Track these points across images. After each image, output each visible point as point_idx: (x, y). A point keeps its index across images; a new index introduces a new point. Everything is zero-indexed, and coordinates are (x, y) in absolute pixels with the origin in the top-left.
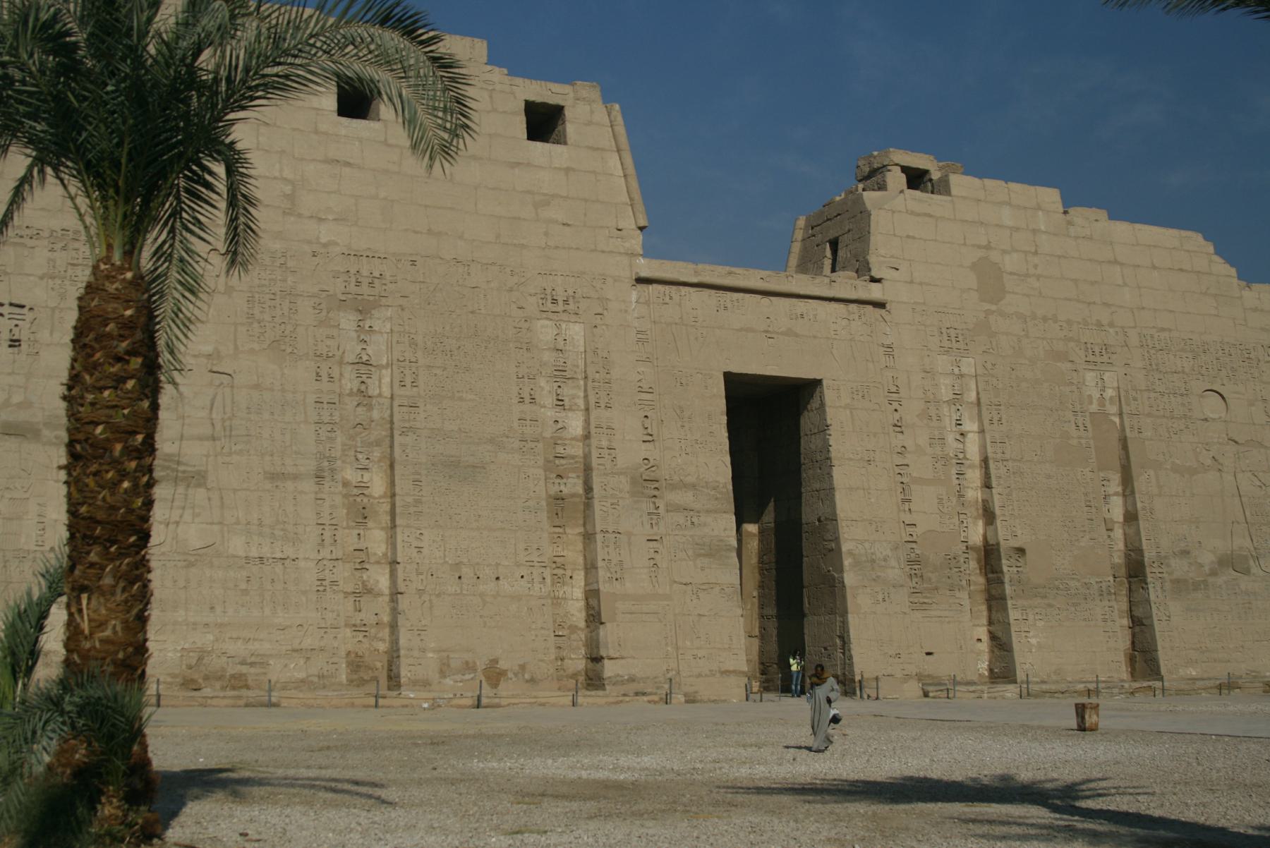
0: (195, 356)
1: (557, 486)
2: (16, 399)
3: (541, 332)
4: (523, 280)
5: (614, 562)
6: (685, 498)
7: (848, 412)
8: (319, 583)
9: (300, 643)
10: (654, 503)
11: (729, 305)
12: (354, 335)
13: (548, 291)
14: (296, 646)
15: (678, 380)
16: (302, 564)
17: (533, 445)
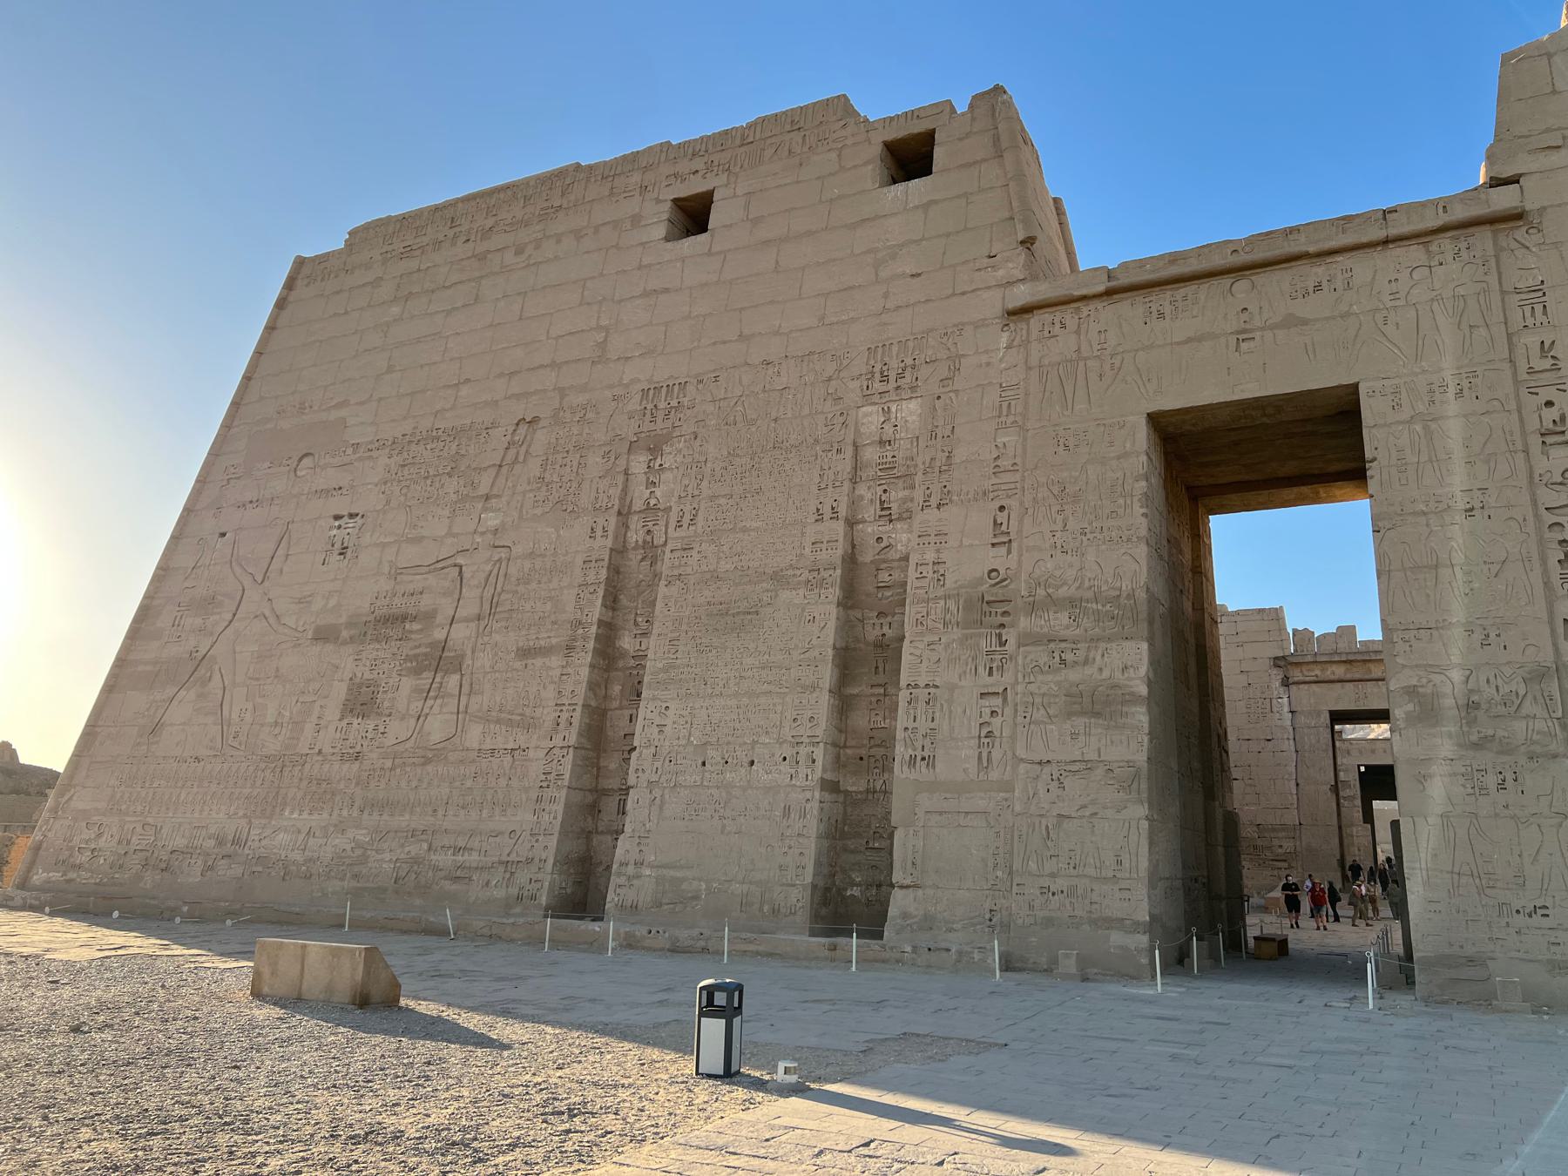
0: (483, 533)
1: (877, 627)
2: (332, 603)
3: (863, 424)
4: (845, 363)
5: (922, 731)
6: (1059, 621)
7: (1418, 428)
8: (543, 777)
9: (508, 855)
10: (999, 636)
11: (1167, 309)
12: (644, 479)
13: (877, 369)
14: (505, 858)
15: (1062, 440)
16: (531, 754)
17: (825, 574)
